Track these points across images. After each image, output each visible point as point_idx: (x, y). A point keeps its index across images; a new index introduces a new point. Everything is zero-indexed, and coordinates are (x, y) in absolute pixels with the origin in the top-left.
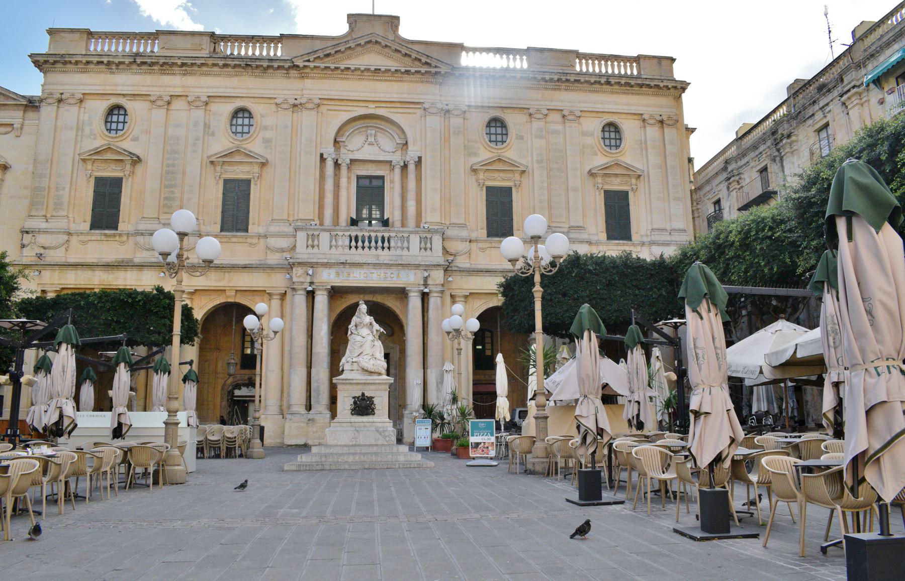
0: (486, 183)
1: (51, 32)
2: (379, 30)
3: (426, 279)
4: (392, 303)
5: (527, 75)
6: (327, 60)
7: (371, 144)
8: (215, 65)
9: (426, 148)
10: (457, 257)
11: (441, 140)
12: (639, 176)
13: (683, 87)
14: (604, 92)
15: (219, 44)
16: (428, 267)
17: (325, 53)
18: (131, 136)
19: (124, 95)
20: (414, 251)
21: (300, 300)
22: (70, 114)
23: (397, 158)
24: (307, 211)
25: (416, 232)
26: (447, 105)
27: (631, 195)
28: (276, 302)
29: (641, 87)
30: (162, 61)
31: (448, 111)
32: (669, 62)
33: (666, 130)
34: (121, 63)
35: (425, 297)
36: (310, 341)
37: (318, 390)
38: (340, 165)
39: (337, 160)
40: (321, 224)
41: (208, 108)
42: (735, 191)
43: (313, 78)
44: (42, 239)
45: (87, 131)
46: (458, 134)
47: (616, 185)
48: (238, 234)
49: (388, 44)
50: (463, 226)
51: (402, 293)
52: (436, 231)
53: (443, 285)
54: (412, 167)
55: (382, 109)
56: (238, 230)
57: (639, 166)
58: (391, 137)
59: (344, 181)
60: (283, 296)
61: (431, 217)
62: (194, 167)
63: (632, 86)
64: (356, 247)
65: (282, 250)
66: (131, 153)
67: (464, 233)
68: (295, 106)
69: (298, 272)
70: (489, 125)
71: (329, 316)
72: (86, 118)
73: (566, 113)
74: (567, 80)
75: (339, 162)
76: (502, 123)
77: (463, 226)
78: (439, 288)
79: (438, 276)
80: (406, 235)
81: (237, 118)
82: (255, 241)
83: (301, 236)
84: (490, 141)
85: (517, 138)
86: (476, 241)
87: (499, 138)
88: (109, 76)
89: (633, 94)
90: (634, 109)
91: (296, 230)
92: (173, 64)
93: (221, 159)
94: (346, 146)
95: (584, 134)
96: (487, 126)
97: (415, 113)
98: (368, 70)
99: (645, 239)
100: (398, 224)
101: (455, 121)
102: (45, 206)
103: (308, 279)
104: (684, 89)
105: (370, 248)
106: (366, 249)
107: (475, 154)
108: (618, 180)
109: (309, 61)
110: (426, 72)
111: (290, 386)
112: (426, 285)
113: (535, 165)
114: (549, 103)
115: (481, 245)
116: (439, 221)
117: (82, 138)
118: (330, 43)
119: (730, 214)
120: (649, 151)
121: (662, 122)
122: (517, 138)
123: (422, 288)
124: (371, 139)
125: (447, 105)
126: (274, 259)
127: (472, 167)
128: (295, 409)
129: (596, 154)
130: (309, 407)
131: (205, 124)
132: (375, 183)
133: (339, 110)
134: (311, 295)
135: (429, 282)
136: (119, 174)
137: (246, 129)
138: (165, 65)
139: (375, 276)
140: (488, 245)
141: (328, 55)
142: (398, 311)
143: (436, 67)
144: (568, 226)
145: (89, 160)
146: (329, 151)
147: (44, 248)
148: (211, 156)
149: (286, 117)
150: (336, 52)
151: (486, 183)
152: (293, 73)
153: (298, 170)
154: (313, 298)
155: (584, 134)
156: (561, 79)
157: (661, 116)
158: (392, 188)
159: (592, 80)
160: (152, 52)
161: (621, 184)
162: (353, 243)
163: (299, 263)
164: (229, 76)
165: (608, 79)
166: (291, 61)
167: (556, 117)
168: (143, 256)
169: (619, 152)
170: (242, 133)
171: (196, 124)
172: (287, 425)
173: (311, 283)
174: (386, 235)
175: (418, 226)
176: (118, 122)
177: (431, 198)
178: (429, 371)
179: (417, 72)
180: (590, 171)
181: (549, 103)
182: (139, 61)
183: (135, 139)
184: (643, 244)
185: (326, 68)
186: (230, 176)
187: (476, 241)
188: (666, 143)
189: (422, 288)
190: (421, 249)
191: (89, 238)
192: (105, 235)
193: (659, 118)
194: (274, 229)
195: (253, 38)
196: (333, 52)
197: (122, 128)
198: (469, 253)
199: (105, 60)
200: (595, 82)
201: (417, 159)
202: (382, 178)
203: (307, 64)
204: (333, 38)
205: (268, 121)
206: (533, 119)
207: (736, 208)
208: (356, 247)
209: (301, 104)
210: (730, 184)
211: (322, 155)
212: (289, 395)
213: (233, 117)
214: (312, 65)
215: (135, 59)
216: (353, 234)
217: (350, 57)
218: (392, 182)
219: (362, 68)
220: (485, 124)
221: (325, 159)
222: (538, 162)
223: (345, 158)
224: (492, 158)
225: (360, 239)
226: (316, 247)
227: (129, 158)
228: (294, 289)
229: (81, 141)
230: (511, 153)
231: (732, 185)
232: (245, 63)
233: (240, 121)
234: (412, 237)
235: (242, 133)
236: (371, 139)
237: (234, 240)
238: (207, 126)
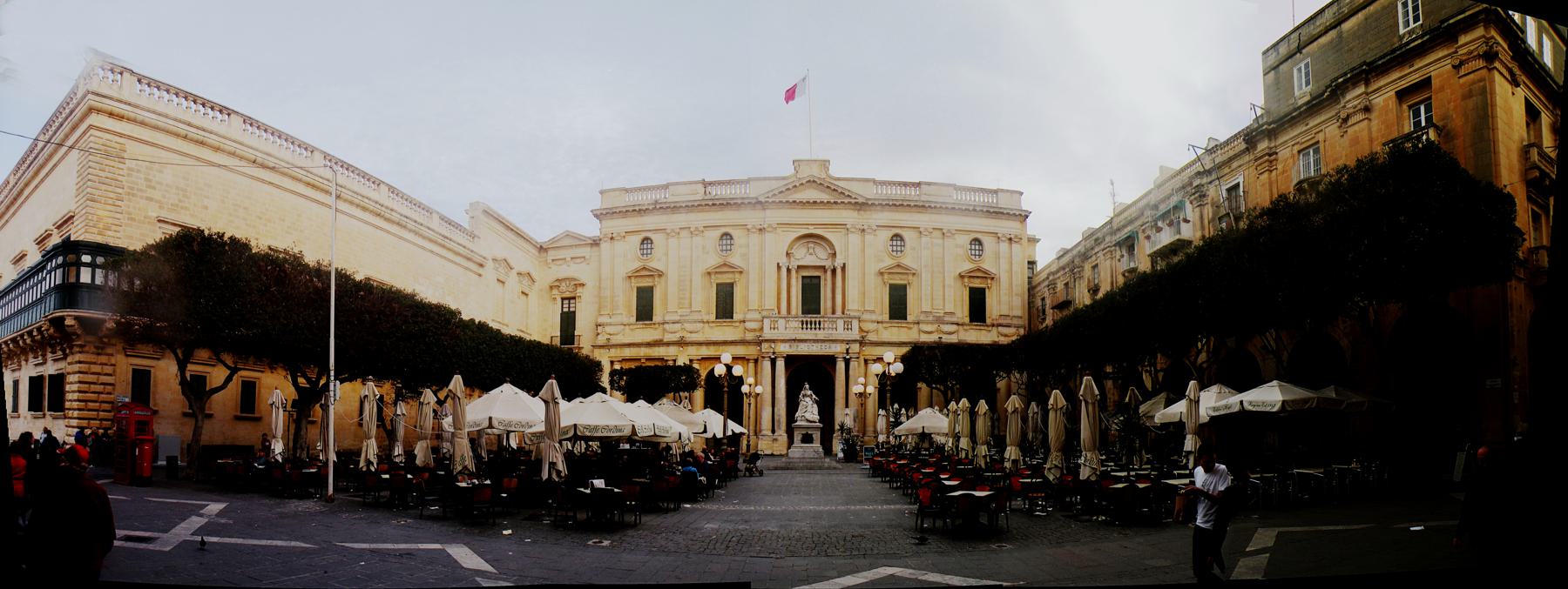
1: (602, 192)
2: (816, 172)
3: (847, 350)
7: (811, 254)
16: (848, 342)
19: (650, 231)
20: (840, 333)
21: (767, 365)
22: (619, 246)
23: (828, 264)
24: (770, 303)
25: (842, 318)
27: (987, 291)
28: (751, 365)
30: (673, 205)
31: (863, 230)
33: (1013, 245)
34: (647, 209)
35: (847, 362)
37: (779, 421)
40: (779, 313)
41: (704, 234)
44: (608, 329)
47: (977, 284)
50: (873, 312)
52: (855, 318)
53: (859, 353)
56: (727, 318)
59: (793, 281)
60: (756, 361)
61: (853, 306)
65: (754, 330)
67: (874, 317)
68: (760, 230)
69: (765, 346)
70: (892, 240)
77: (873, 312)
78: (856, 356)
79: (855, 348)
82: (738, 324)
83: (767, 322)
86: (882, 322)
87: (899, 249)
88: (639, 218)
91: (763, 318)
98: (808, 202)
99: (995, 322)
105: (811, 329)
107: (882, 261)
108: (979, 280)
109: (768, 197)
111: (761, 418)
112: (848, 353)
115: (885, 325)
121: (1010, 239)
123: (845, 355)
124: (811, 251)
126: (750, 336)
128: (764, 432)
130: (773, 431)
132: (815, 281)
134: (773, 362)
135: (850, 351)
136: (650, 284)
137: (729, 247)
138: (674, 208)
139: (814, 348)
140: (890, 325)
143: (855, 198)
146: (783, 261)
149: (755, 238)
152: (759, 206)
155: (957, 246)
158: (825, 284)
160: (665, 198)
163: (767, 341)
166: (757, 199)
170: (726, 250)
172: (760, 442)
173: (774, 353)
175: (843, 313)
176: (647, 249)
183: (659, 260)
184: (993, 325)
187: (882, 322)
189: (845, 355)
191: (635, 327)
192: (646, 324)
196: (784, 190)
198: (877, 331)
199: (637, 208)
202: (819, 277)
204: (784, 178)
211: (778, 264)
212: (760, 424)
217: (795, 192)
218: (825, 280)
228: (763, 357)
233: (724, 242)
234: (839, 320)
235: (726, 250)
236: (811, 251)
237: (725, 324)
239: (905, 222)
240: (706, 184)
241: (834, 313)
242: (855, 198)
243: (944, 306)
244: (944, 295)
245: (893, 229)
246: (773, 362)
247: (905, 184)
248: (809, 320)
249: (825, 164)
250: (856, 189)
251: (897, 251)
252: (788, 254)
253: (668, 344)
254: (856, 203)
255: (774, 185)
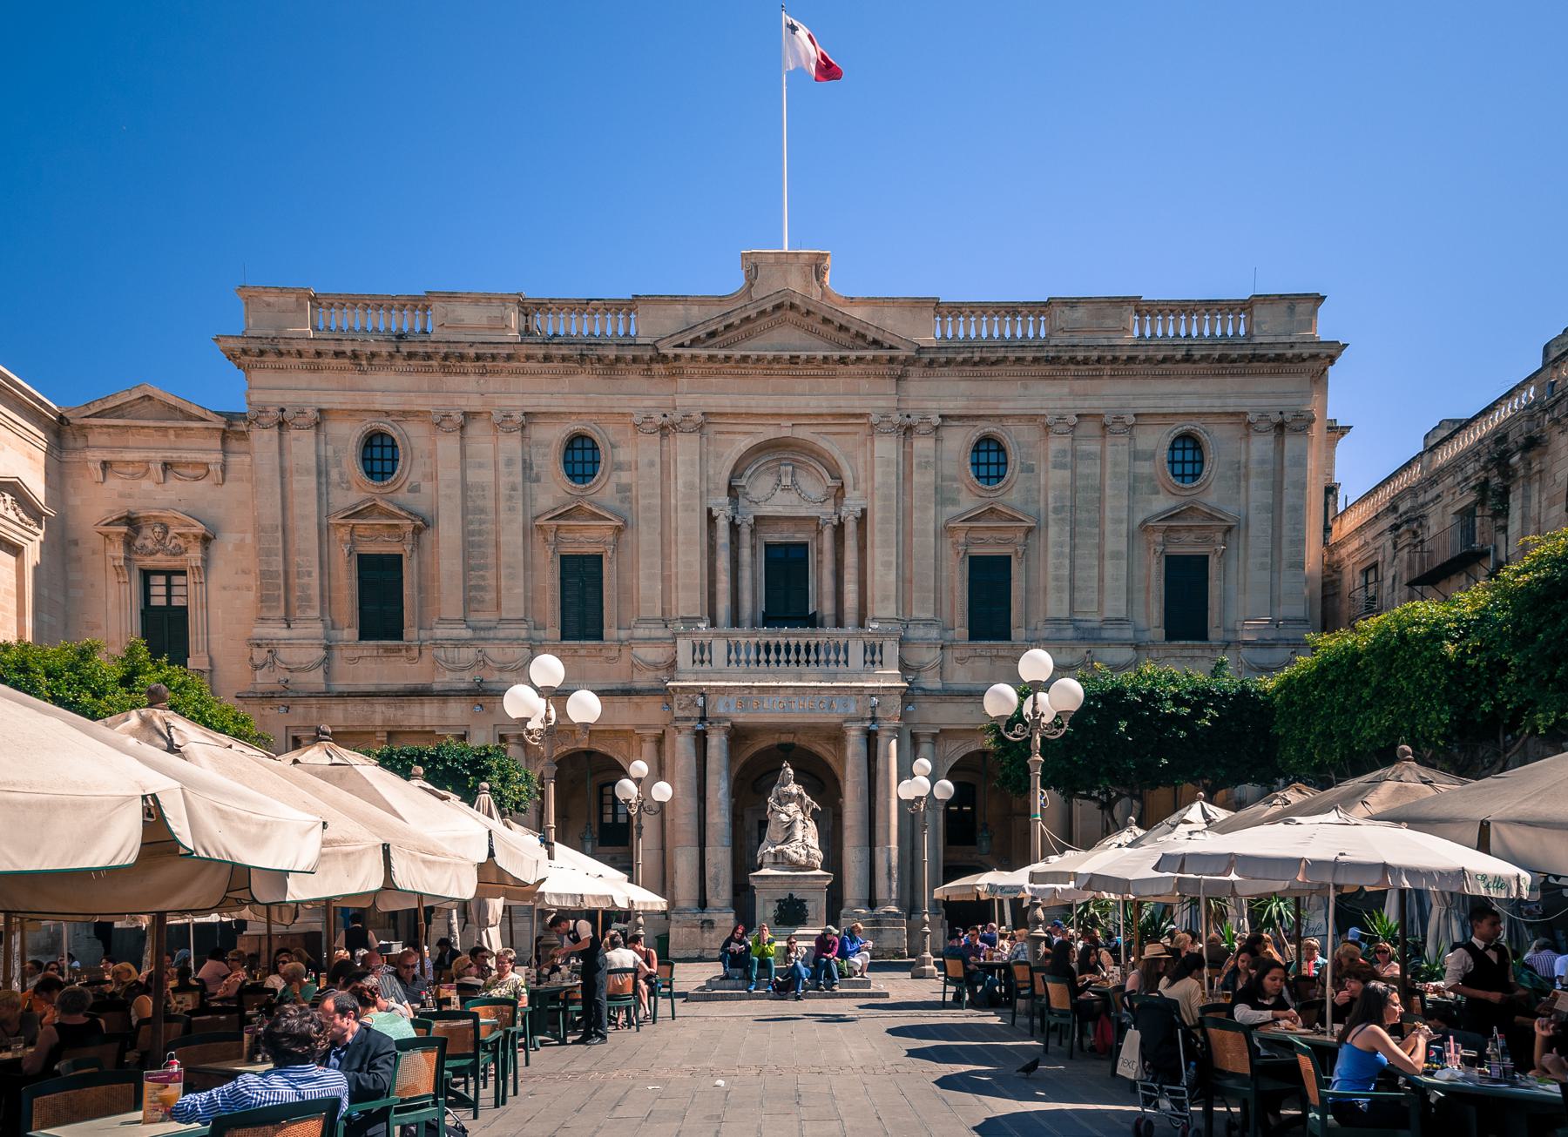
0: (969, 551)
4: (823, 749)
5: (1045, 354)
6: (711, 342)
7: (786, 489)
8: (529, 358)
9: (872, 493)
10: (923, 674)
11: (898, 479)
12: (1229, 529)
13: (1330, 353)
14: (1181, 376)
15: (533, 317)
17: (709, 330)
18: (407, 484)
21: (682, 746)
23: (826, 511)
24: (689, 601)
26: (908, 416)
29: (1250, 361)
32: (1310, 305)
36: (702, 805)
37: (716, 878)
38: (739, 526)
39: (734, 518)
42: (1406, 550)
43: (691, 376)
45: (334, 475)
46: (926, 468)
47: (1187, 546)
48: (588, 642)
49: (811, 309)
51: (836, 736)
54: (851, 528)
55: (802, 427)
56: (587, 637)
57: (1231, 510)
58: (818, 475)
62: (512, 537)
63: (1234, 361)
64: (768, 662)
65: (655, 666)
66: (411, 513)
68: (663, 428)
70: (976, 449)
71: (730, 770)
72: (331, 453)
73: (1107, 419)
74: (1115, 359)
75: (738, 521)
76: (999, 444)
80: (842, 641)
81: (573, 449)
84: (978, 477)
85: (1022, 471)
87: (993, 471)
89: (1232, 375)
90: (1232, 404)
92: (462, 357)
93: (552, 522)
94: (747, 494)
95: (1136, 456)
96: (973, 451)
97: (856, 433)
100: (829, 620)
101: (923, 445)
102: (283, 603)
103: (697, 713)
104: (1332, 360)
106: (783, 665)
107: (954, 502)
108: (1192, 537)
109: (682, 345)
110: (875, 360)
113: (1051, 516)
114: (1079, 403)
116: (895, 616)
117: (327, 488)
118: (716, 311)
119: (1393, 591)
120: (1252, 481)
122: (1022, 471)
124: (787, 481)
125: (908, 416)
126: (643, 680)
127: (947, 522)
129: (1157, 493)
131: (524, 461)
133: (734, 433)
134: (701, 739)
136: (394, 549)
141: (712, 335)
142: (831, 760)
143: (891, 347)
144: (1100, 619)
145: (343, 525)
147: (291, 671)
148: (537, 517)
150: (727, 327)
151: (969, 551)
152: (658, 368)
153: (673, 537)
154: (705, 742)
156: (1104, 357)
157: (1281, 413)
158: (820, 562)
159: (1161, 355)
161: (1196, 544)
162: (763, 656)
164: (556, 375)
165: (1189, 350)
166: (654, 346)
167: (1091, 427)
168: (447, 679)
169: (1201, 485)
171: (510, 462)
174: (813, 642)
177: (883, 576)
178: (877, 849)
179: (859, 359)
180: (1145, 521)
181: (1079, 403)
182: (405, 349)
185: (711, 358)
186: (569, 550)
188: (1286, 463)
190: (865, 662)
192: (387, 649)
193: (1276, 418)
194: (640, 632)
195: (588, 304)
197: (390, 470)
200: (1165, 360)
201: (859, 515)
203: (679, 351)
204: (721, 299)
205: (623, 455)
206: (1051, 435)
207: (1405, 580)
208: (768, 662)
209: (673, 426)
210: (1399, 536)
211: (710, 511)
212: (673, 886)
213: (567, 449)
214: (687, 352)
215: (398, 348)
216: (763, 641)
217: (748, 336)
218: (820, 551)
219: (770, 354)
220: (971, 447)
221: (716, 518)
222: (1056, 510)
223: (746, 520)
224: (980, 507)
225: (773, 648)
226: (706, 663)
227: (409, 522)
229: (328, 494)
230: (1012, 494)
231: (1403, 538)
232: (579, 352)
238: (527, 466)
239: (1011, 404)
240: (529, 309)
241: (839, 622)
242: (891, 347)
243: (1100, 604)
244: (1101, 579)
245: (980, 424)
246: (701, 739)
247: (1012, 310)
248: (782, 641)
249: (817, 267)
250: (894, 325)
251: (988, 477)
252: (732, 491)
253: (445, 695)
254: (892, 360)
255: (696, 314)
